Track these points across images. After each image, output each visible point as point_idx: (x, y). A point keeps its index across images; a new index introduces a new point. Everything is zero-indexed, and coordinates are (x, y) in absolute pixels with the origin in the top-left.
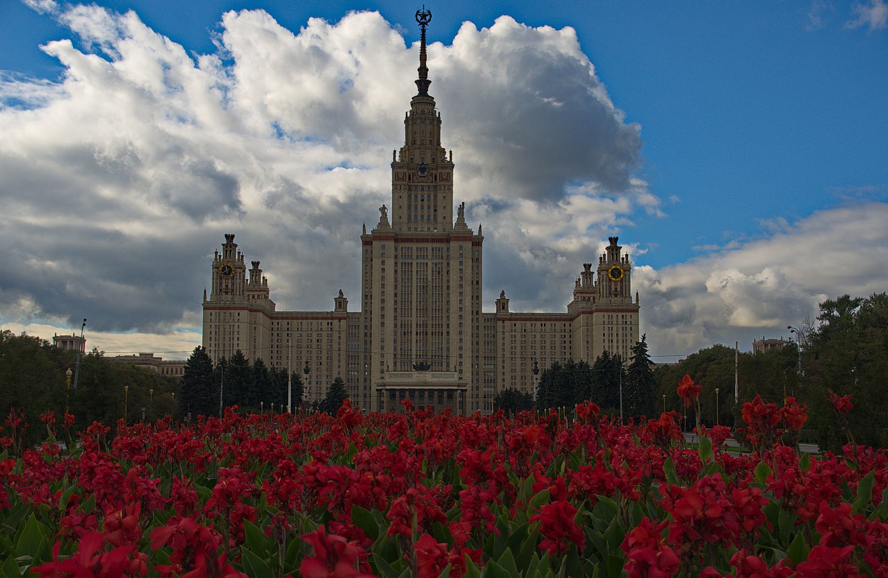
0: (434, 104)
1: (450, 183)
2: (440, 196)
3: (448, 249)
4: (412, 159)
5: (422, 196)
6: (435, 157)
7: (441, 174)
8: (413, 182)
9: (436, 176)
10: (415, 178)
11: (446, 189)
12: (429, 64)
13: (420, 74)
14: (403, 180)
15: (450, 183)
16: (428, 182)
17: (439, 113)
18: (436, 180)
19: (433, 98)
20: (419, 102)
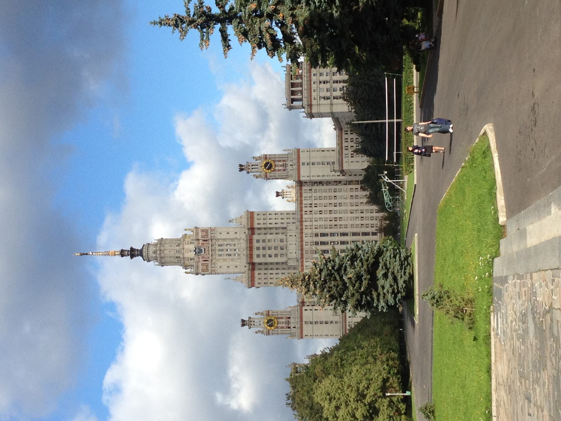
1: (209, 231)
2: (219, 236)
3: (259, 229)
4: (191, 259)
6: (189, 243)
7: (202, 237)
8: (209, 258)
10: (206, 257)
14: (208, 266)
15: (209, 231)
17: (155, 240)
18: (206, 241)
19: (144, 245)
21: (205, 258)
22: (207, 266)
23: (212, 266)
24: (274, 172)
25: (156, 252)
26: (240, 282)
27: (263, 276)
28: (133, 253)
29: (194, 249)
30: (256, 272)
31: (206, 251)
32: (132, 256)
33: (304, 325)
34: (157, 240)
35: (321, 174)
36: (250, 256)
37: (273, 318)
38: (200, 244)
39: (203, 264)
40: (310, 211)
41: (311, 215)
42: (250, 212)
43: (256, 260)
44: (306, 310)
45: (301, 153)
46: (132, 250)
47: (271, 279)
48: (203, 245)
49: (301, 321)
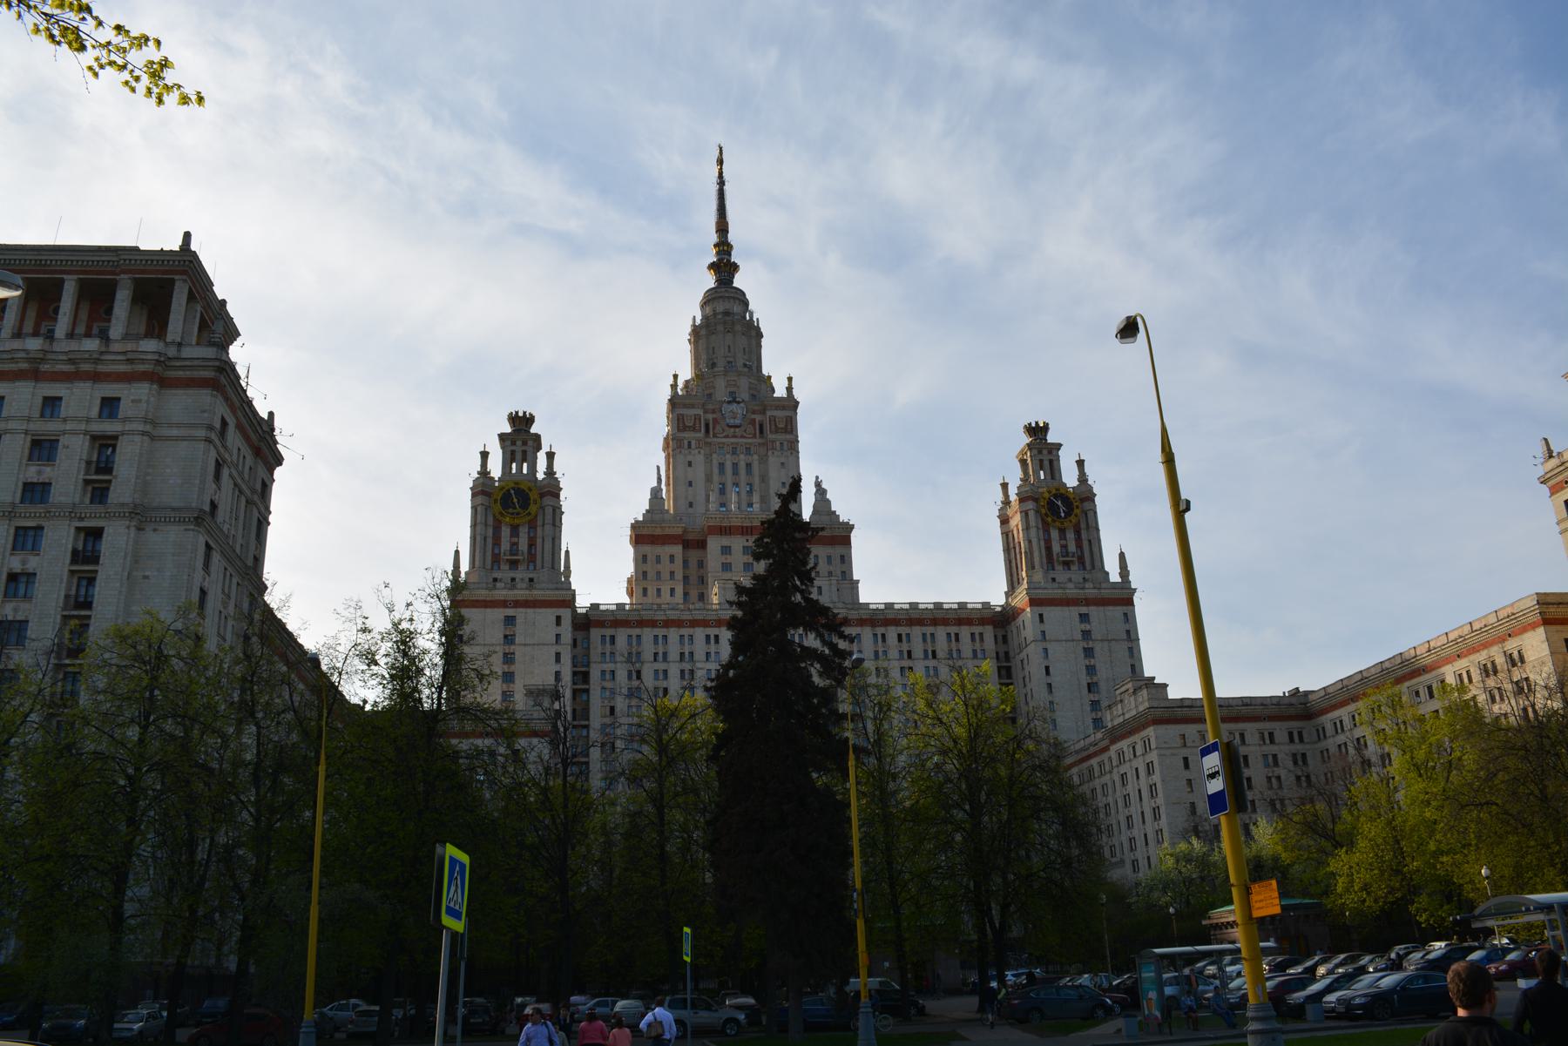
0: (746, 303)
1: (788, 437)
4: (710, 395)
5: (735, 466)
6: (755, 393)
7: (773, 420)
8: (715, 436)
9: (761, 426)
10: (718, 428)
11: (785, 447)
12: (732, 237)
13: (718, 253)
16: (745, 437)
17: (758, 319)
18: (761, 432)
20: (721, 297)
21: (714, 428)
22: (693, 429)
23: (693, 443)
24: (1040, 526)
25: (728, 316)
26: (648, 508)
27: (665, 567)
28: (724, 268)
29: (737, 399)
30: (677, 550)
31: (732, 430)
32: (712, 266)
33: (499, 614)
34: (758, 324)
35: (1056, 679)
36: (725, 527)
37: (533, 508)
38: (753, 416)
39: (700, 419)
40: (909, 653)
41: (897, 655)
42: (850, 536)
43: (714, 544)
44: (558, 619)
45: (1118, 611)
46: (735, 267)
47: (659, 590)
48: (750, 423)
49: (518, 604)
